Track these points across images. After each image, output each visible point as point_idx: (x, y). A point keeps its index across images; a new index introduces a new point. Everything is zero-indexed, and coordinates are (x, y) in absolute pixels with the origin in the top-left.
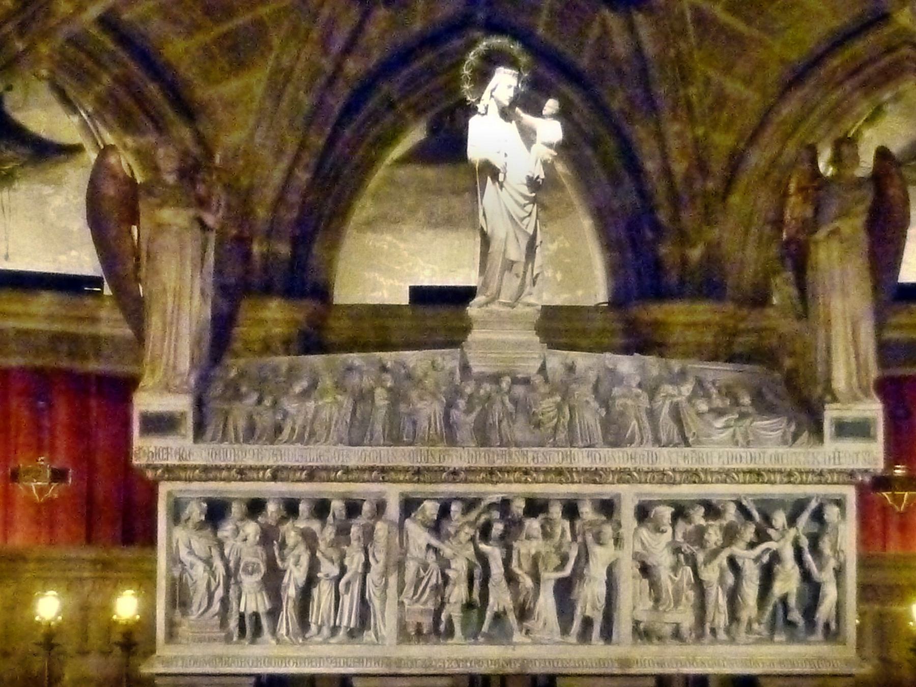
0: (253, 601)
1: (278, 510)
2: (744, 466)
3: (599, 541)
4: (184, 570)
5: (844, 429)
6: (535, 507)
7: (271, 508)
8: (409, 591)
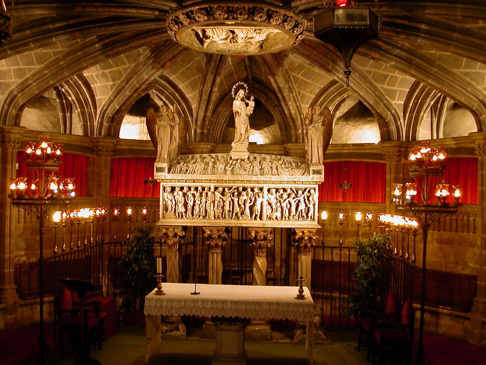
0: (181, 209)
3: (258, 196)
4: (166, 202)
5: (314, 172)
6: (245, 189)
7: (185, 188)
8: (216, 207)
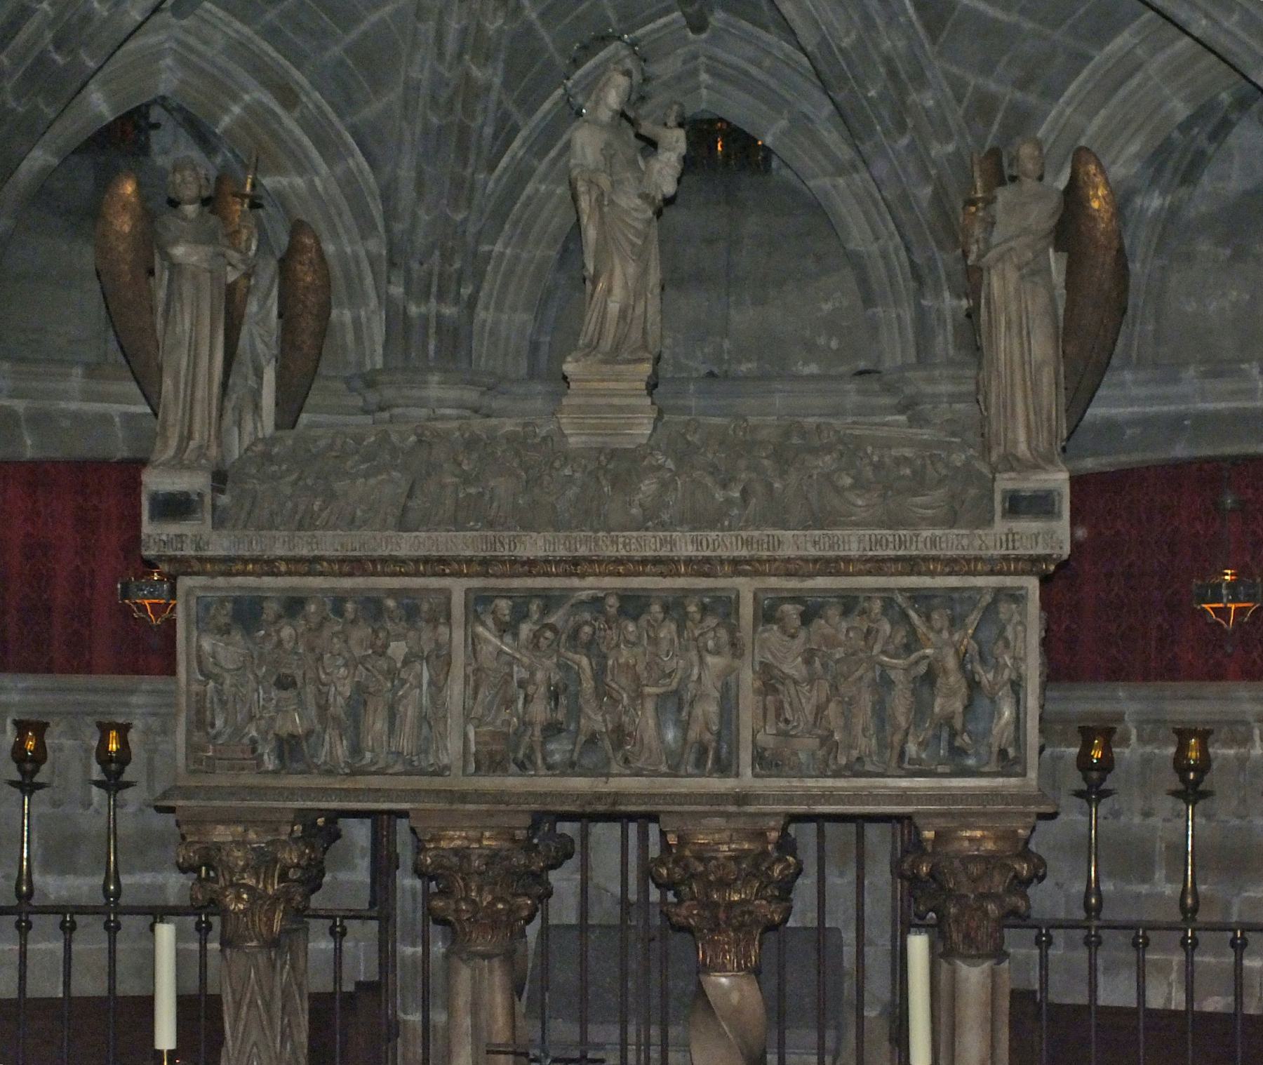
5: (1017, 505)
6: (633, 605)
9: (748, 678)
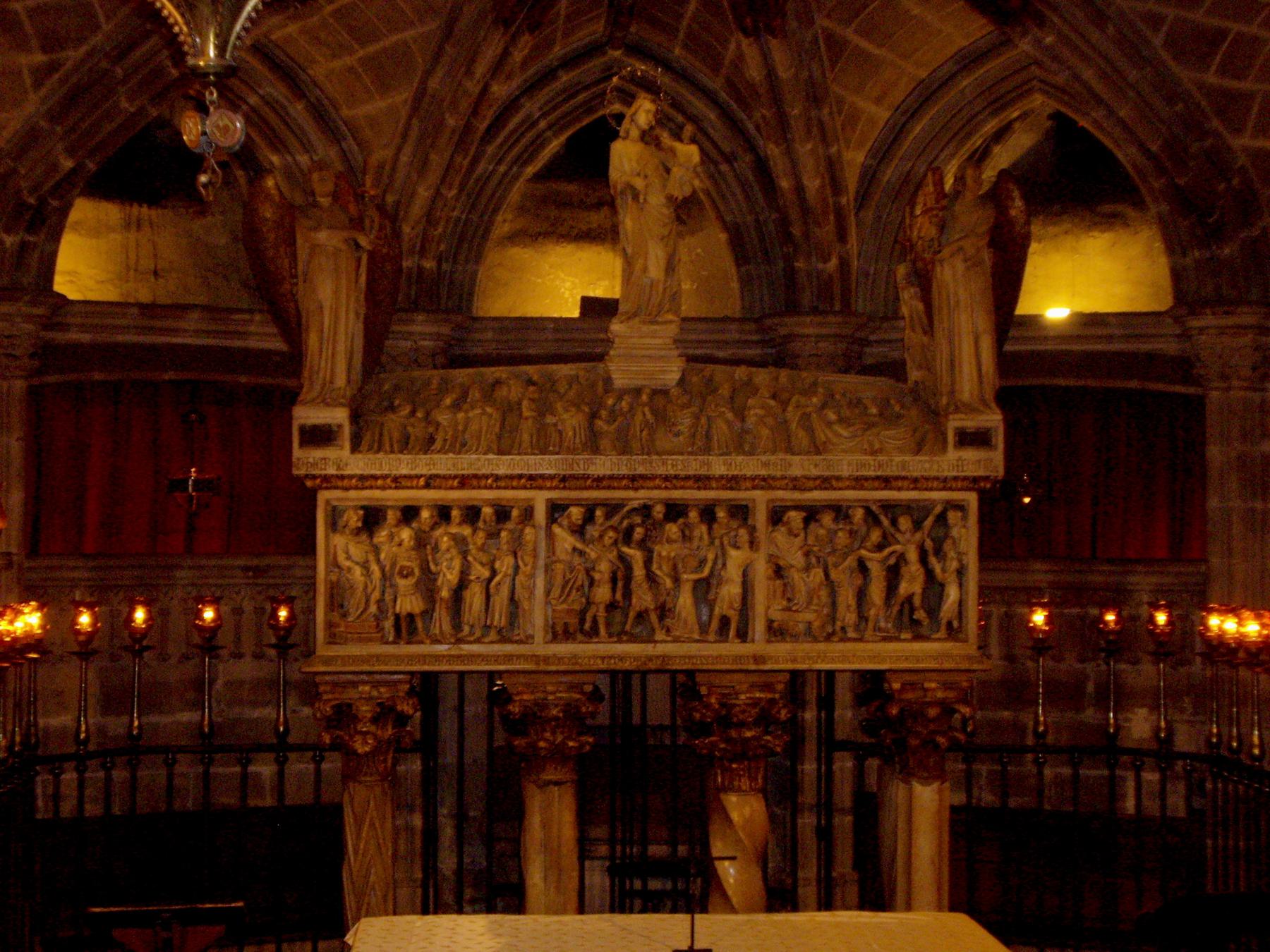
1: (432, 516)
2: (872, 473)
6: (675, 511)
7: (425, 514)
8: (556, 592)
9: (761, 570)
